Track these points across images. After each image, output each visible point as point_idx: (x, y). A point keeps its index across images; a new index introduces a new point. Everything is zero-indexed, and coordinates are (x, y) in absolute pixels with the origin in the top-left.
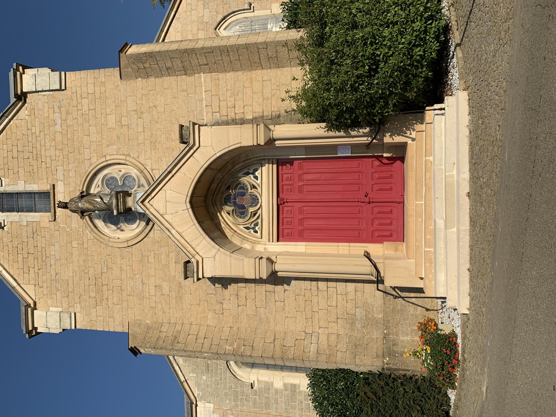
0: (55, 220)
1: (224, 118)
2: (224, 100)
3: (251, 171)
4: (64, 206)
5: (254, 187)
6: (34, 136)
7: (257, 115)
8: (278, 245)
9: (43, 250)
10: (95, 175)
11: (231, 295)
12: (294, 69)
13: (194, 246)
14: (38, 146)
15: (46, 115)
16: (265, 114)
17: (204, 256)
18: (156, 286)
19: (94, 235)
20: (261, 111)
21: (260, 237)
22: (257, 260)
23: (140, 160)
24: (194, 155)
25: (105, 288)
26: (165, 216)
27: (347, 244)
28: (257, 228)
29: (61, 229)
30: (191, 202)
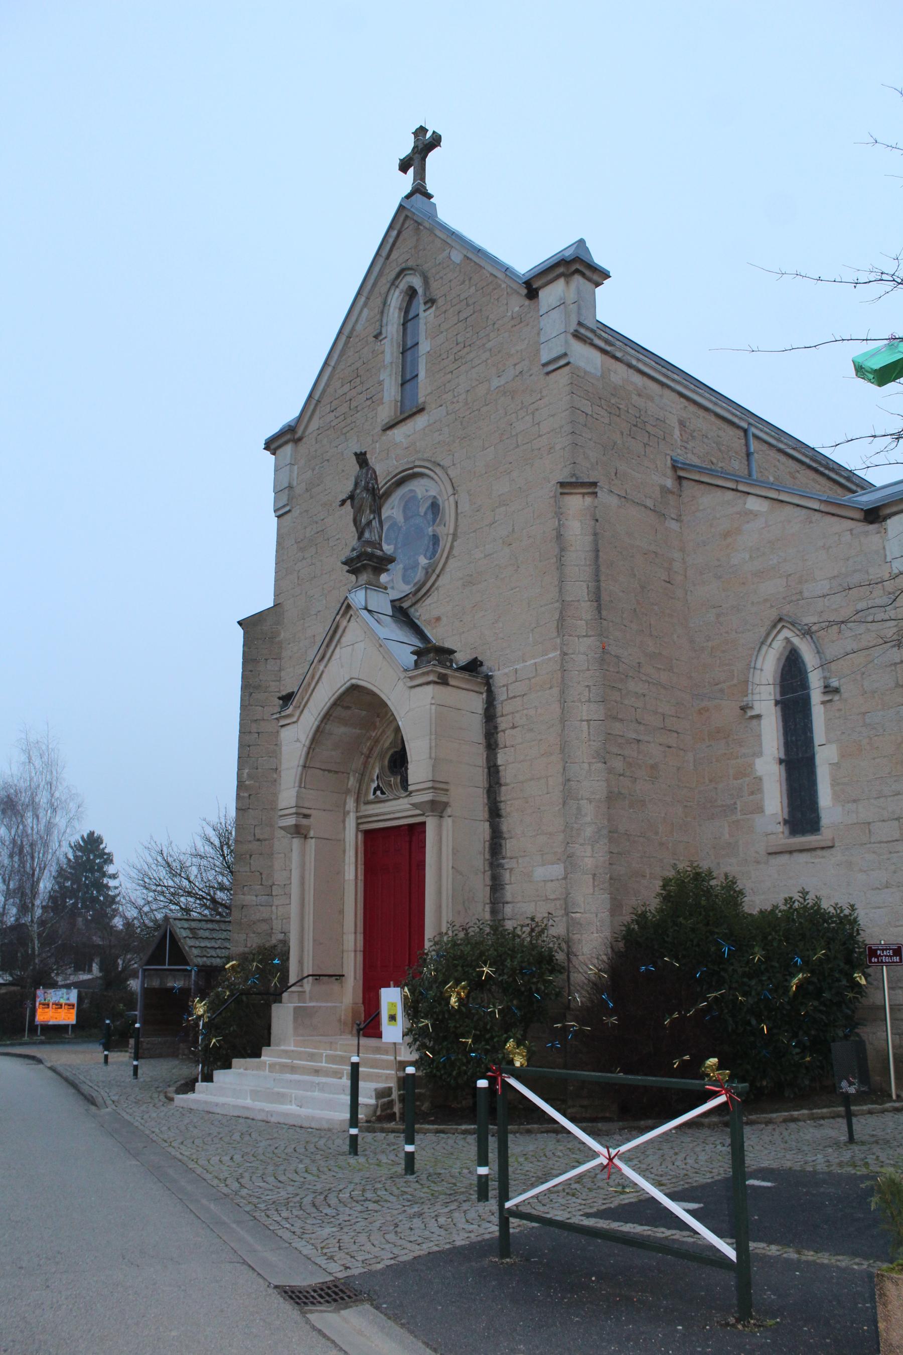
7: (502, 774)
16: (503, 788)
20: (508, 781)
23: (451, 561)
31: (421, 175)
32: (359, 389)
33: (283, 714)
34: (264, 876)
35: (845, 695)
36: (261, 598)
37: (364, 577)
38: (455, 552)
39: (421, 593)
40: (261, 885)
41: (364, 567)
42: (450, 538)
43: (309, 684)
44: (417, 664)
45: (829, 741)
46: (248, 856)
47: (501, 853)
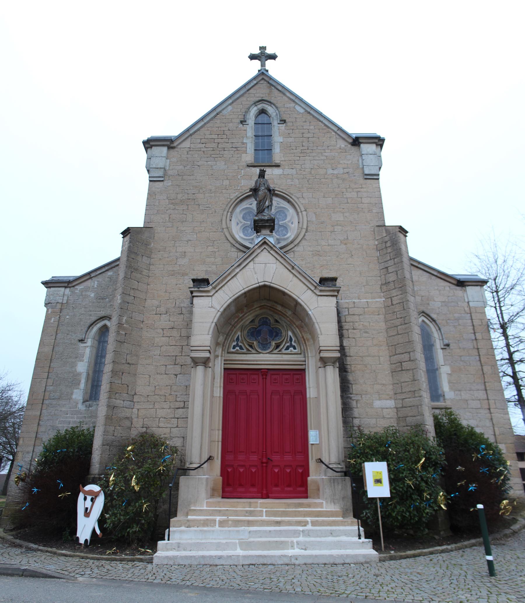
0: (248, 166)
1: (343, 319)
2: (359, 319)
3: (293, 343)
4: (262, 175)
5: (277, 346)
6: (322, 151)
7: (347, 350)
8: (221, 368)
9: (222, 156)
10: (289, 201)
11: (174, 322)
12: (391, 387)
13: (223, 288)
14: (314, 154)
15: (341, 162)
16: (348, 358)
17: (213, 297)
18: (185, 252)
19: (234, 199)
20: (351, 355)
21: (229, 351)
22: (208, 348)
23: (303, 241)
24: (309, 290)
25: (185, 207)
26: (252, 262)
27: (220, 439)
28: (238, 348)
29: (239, 170)
30: (265, 286)
33: (201, 289)
34: (130, 388)
40: (127, 394)
42: (304, 230)
43: (226, 277)
46: (121, 373)
47: (349, 391)
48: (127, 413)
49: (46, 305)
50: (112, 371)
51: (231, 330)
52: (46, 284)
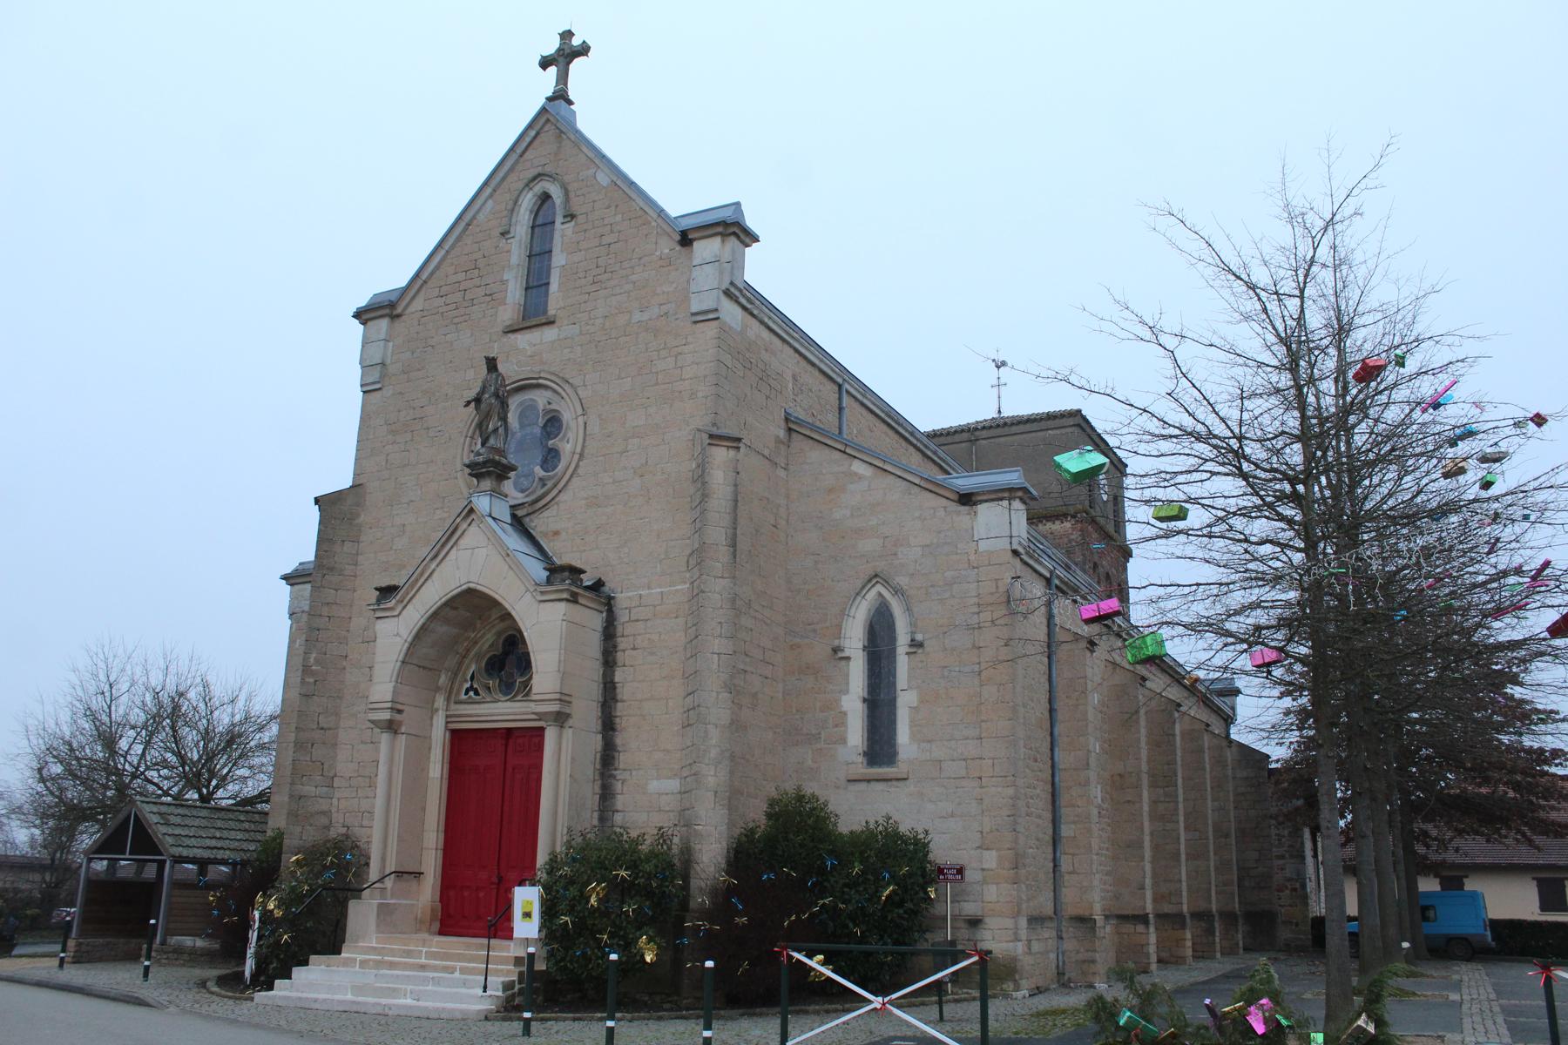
23: (574, 480)
30: (470, 591)
31: (563, 78)
32: (477, 281)
35: (928, 649)
36: (343, 480)
37: (487, 484)
38: (580, 471)
39: (537, 505)
41: (489, 474)
44: (549, 581)
45: (910, 688)
48: (323, 805)
49: (291, 615)
50: (296, 743)
51: (460, 663)
52: (286, 578)
